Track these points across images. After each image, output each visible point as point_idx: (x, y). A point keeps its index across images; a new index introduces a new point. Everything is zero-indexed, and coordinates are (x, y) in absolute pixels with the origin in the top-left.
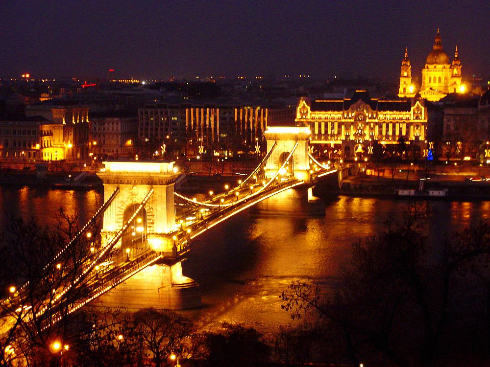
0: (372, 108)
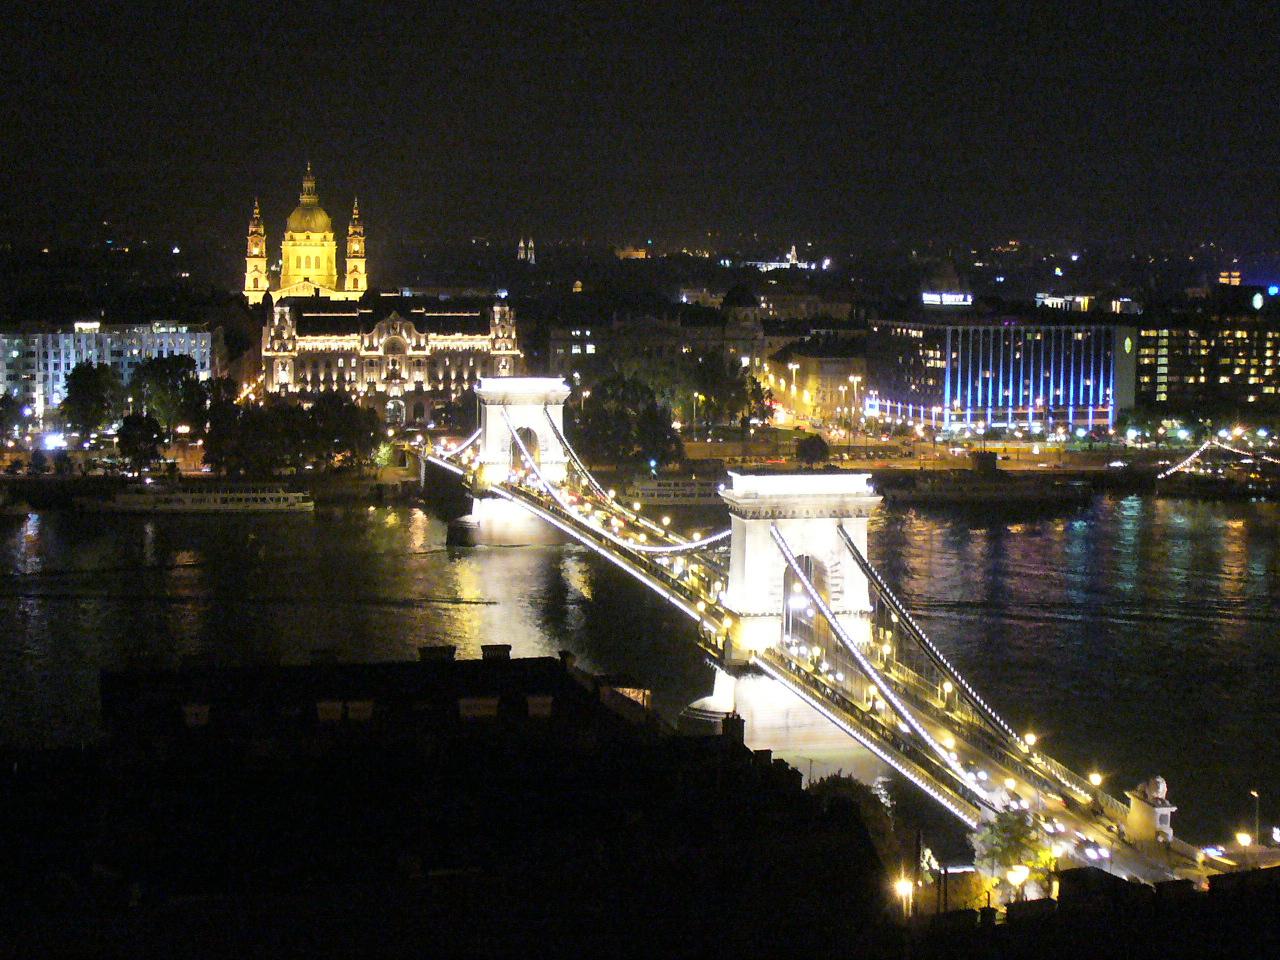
0: (417, 329)
